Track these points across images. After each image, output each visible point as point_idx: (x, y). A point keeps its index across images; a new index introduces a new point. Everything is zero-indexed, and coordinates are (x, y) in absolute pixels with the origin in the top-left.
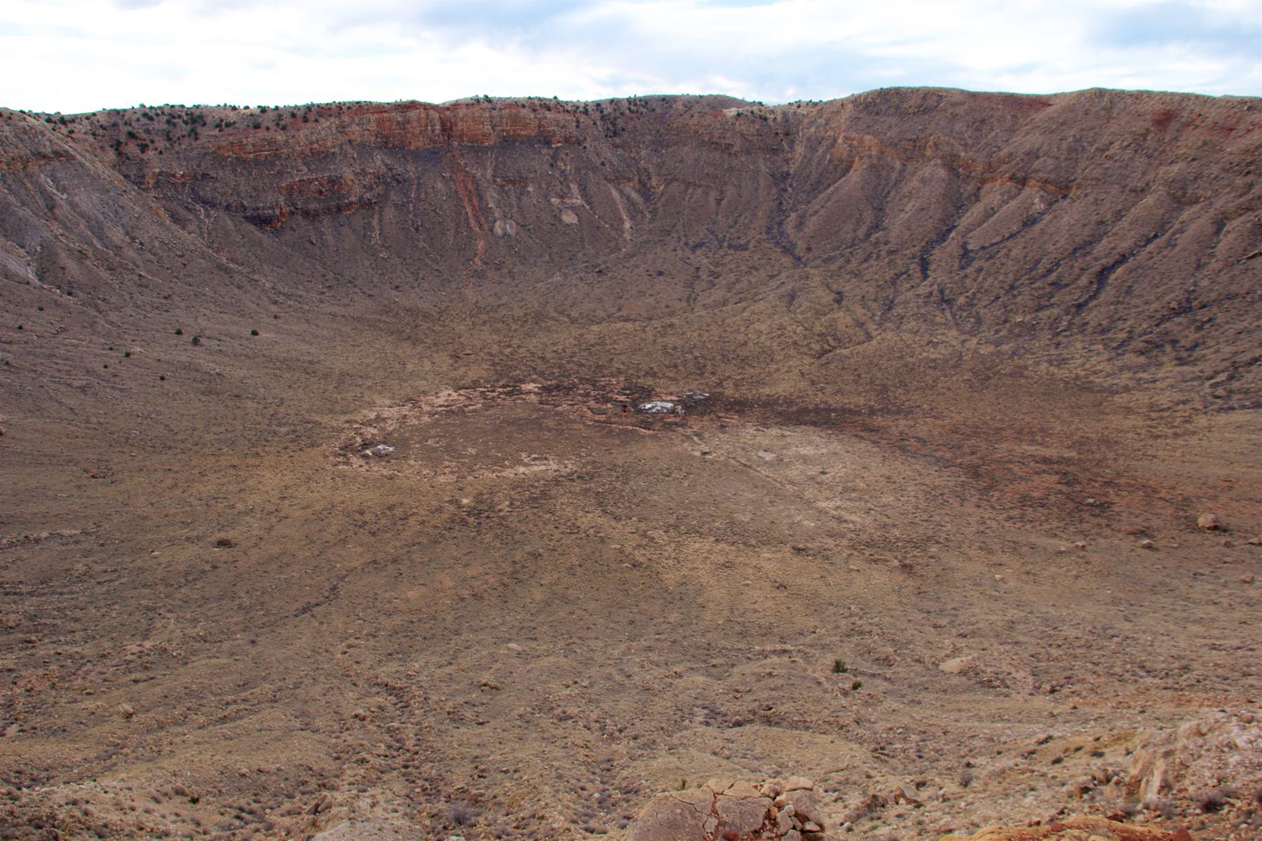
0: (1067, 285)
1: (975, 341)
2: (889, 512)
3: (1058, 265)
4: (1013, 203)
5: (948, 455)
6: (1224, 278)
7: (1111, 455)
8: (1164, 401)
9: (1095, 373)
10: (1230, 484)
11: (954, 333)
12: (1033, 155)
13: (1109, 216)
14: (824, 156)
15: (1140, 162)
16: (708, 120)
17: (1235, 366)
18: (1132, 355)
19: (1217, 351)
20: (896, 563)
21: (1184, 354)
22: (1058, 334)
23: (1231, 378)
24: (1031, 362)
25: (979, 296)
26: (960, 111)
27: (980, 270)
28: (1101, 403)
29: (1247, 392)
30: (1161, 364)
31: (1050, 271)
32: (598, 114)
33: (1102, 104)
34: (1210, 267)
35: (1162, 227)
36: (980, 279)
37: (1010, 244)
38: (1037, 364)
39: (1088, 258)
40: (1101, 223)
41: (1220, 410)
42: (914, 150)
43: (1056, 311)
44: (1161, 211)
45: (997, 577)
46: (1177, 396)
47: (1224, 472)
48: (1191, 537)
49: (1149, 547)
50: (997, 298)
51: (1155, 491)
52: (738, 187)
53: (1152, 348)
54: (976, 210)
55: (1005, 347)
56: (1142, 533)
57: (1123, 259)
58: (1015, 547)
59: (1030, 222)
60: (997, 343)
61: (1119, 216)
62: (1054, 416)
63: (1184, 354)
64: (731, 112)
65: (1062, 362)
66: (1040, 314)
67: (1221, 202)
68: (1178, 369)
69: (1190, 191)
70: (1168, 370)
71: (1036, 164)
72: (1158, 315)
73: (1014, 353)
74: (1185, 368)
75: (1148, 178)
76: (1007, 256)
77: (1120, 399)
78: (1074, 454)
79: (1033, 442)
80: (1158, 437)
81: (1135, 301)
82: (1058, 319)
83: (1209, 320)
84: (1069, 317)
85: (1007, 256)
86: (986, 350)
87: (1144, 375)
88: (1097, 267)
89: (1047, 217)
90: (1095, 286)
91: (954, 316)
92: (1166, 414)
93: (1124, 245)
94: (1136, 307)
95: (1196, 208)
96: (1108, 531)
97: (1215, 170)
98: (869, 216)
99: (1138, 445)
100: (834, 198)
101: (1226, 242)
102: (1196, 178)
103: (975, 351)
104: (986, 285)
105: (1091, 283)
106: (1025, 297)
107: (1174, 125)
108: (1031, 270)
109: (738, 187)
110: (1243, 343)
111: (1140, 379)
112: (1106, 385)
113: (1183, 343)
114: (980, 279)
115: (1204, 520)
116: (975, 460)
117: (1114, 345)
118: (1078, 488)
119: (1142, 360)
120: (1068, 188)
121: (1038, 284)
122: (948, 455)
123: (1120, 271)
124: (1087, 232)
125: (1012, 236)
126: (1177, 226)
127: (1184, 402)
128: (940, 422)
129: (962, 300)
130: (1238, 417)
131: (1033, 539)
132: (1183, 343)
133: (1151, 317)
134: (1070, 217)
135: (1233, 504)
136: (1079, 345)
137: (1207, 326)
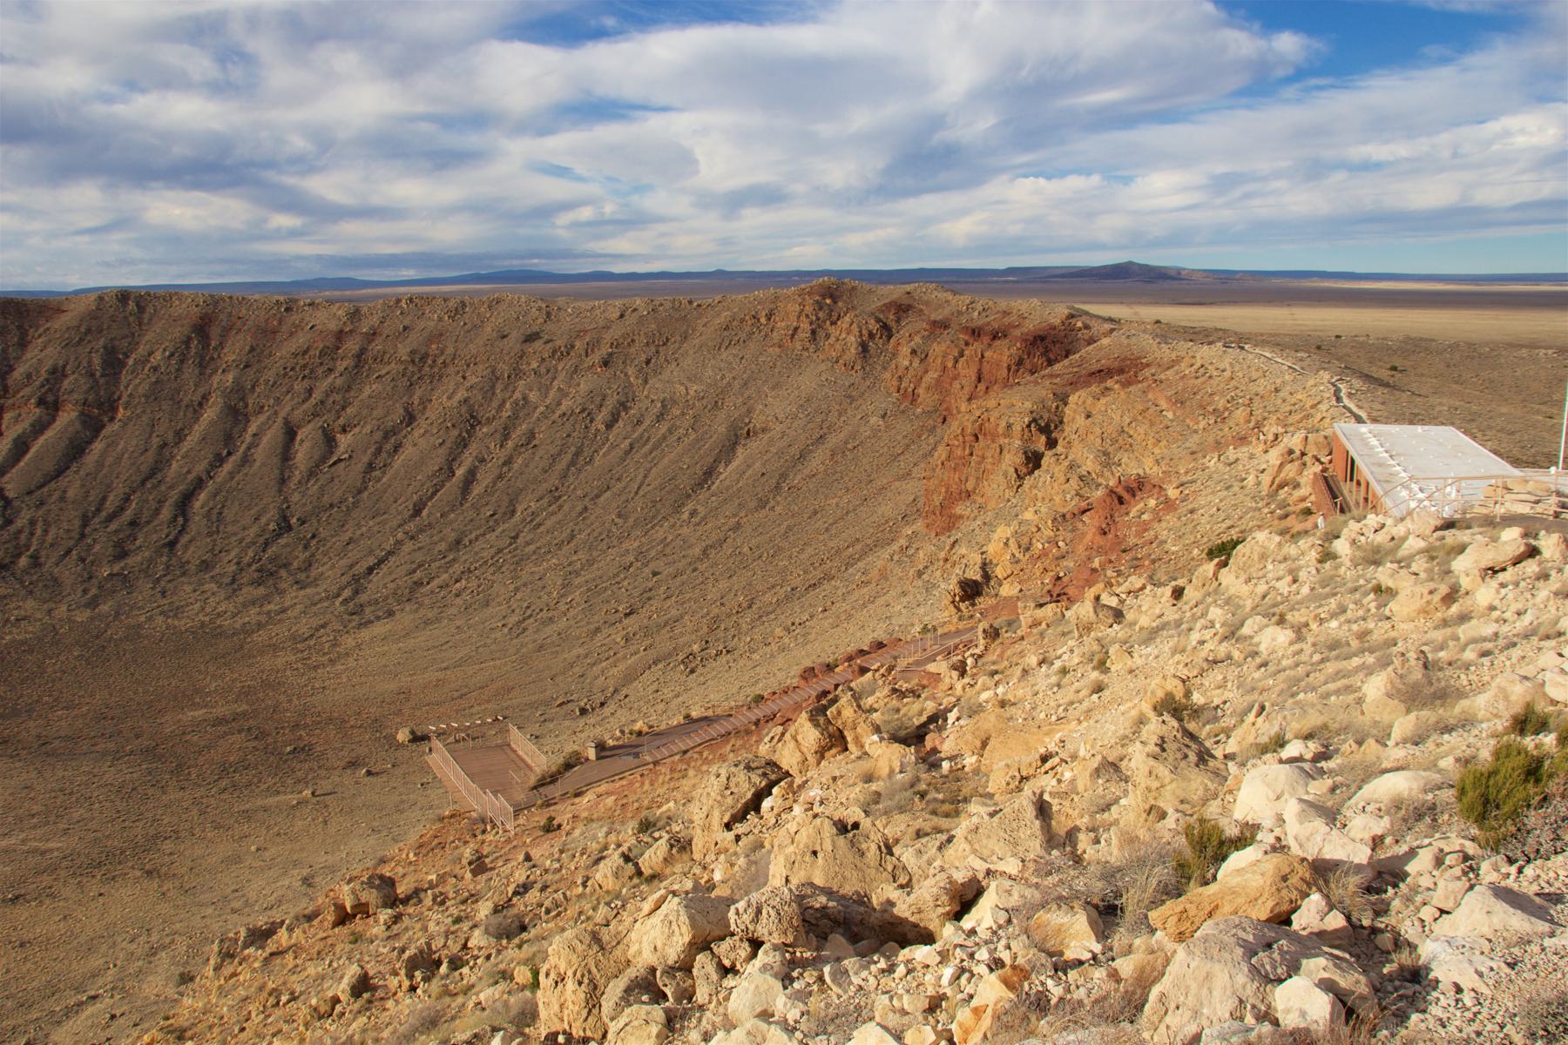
0: (148, 523)
1: (64, 608)
2: (93, 825)
3: (127, 499)
4: (49, 433)
5: (111, 746)
6: (314, 488)
7: (282, 698)
8: (304, 629)
9: (219, 615)
10: (406, 693)
11: (30, 604)
12: (57, 373)
13: (170, 436)
15: (190, 371)
17: (356, 579)
18: (250, 588)
19: (333, 566)
20: (139, 873)
21: (302, 576)
22: (158, 580)
23: (356, 592)
24: (143, 619)
25: (43, 553)
27: (33, 523)
28: (242, 647)
29: (377, 602)
30: (284, 591)
31: (122, 509)
33: (129, 308)
34: (295, 480)
35: (229, 439)
36: (39, 532)
37: (63, 481)
38: (150, 619)
39: (163, 488)
40: (165, 445)
41: (361, 625)
43: (147, 554)
44: (228, 425)
45: (253, 848)
46: (315, 622)
47: (393, 686)
48: (398, 754)
49: (369, 773)
50: (69, 552)
51: (344, 721)
53: (266, 575)
55: (104, 608)
56: (353, 764)
57: (199, 484)
58: (247, 815)
59: (76, 450)
60: (93, 603)
61: (180, 436)
62: (200, 672)
63: (302, 576)
65: (177, 612)
66: (130, 561)
67: (288, 408)
68: (302, 593)
69: (251, 401)
70: (292, 596)
71: (66, 384)
72: (261, 540)
73: (117, 614)
74: (308, 591)
75: (201, 391)
76: (62, 499)
77: (260, 637)
78: (245, 707)
79: (195, 706)
80: (316, 668)
81: (230, 529)
82: (150, 560)
83: (314, 536)
84: (164, 559)
85: (62, 499)
86: (82, 616)
87: (271, 607)
88: (174, 495)
89: (98, 446)
90: (181, 520)
91: (22, 582)
92: (312, 642)
93: (200, 468)
94: (235, 534)
95: (262, 418)
96: (323, 773)
97: (270, 375)
99: (303, 681)
101: (303, 453)
102: (253, 387)
103: (70, 620)
104: (50, 538)
105: (175, 517)
106: (101, 545)
107: (215, 332)
108: (98, 510)
110: (354, 553)
111: (269, 612)
112: (238, 626)
113: (295, 564)
114: (39, 532)
115: (403, 736)
116: (145, 742)
117: (228, 580)
118: (270, 740)
119: (261, 590)
120: (114, 410)
121: (113, 526)
122: (111, 746)
123: (203, 496)
124: (150, 457)
125: (60, 472)
126: (248, 438)
127: (323, 626)
128: (76, 712)
129: (23, 561)
130: (380, 629)
131: (259, 802)
132: (295, 564)
133: (254, 543)
134: (122, 444)
135: (418, 713)
136: (188, 588)
137: (314, 542)
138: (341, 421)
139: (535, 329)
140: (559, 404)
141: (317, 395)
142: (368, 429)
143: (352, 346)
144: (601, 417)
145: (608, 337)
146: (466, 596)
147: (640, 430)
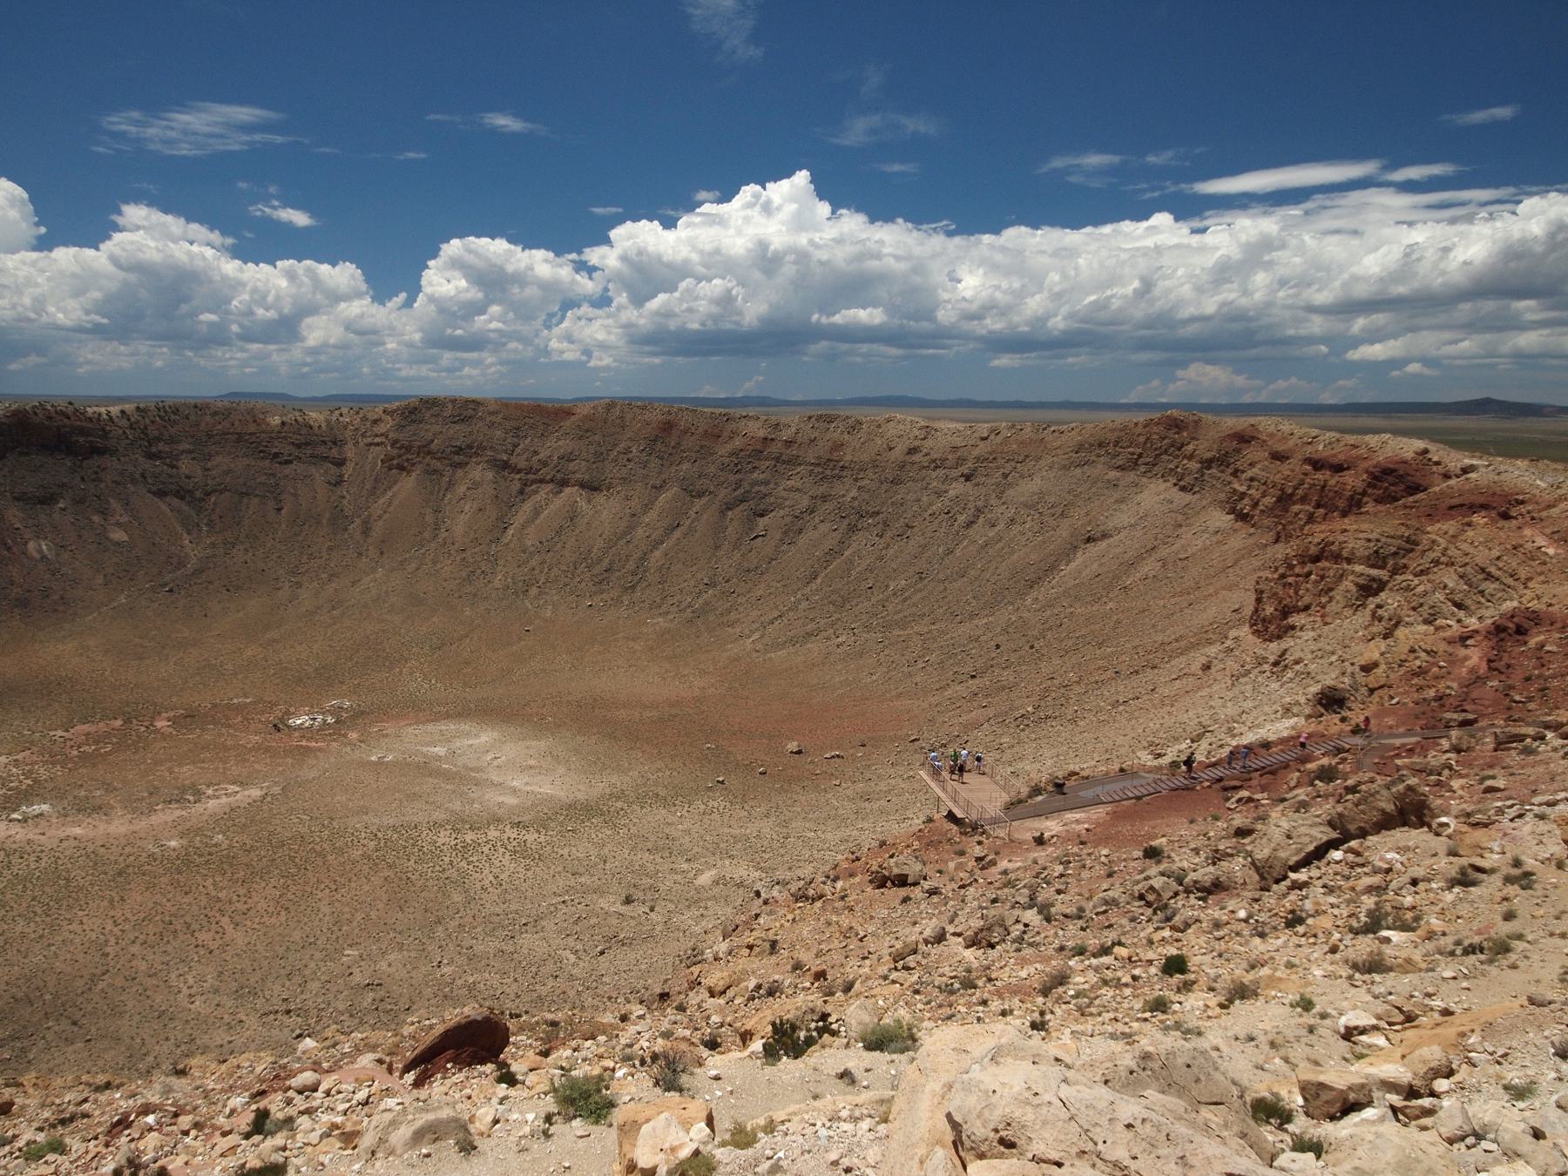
4: (558, 502)
14: (375, 464)
16: (252, 428)
26: (498, 419)
32: (124, 423)
42: (461, 455)
52: (295, 495)
54: (528, 507)
61: (647, 507)
64: (276, 421)
95: (705, 499)
98: (429, 519)
100: (396, 503)
109: (295, 495)
123: (657, 553)
129: (534, 591)
138: (762, 507)
139: (916, 443)
140: (931, 504)
141: (746, 485)
142: (782, 513)
143: (774, 449)
144: (962, 518)
145: (976, 452)
146: (845, 648)
147: (996, 529)
